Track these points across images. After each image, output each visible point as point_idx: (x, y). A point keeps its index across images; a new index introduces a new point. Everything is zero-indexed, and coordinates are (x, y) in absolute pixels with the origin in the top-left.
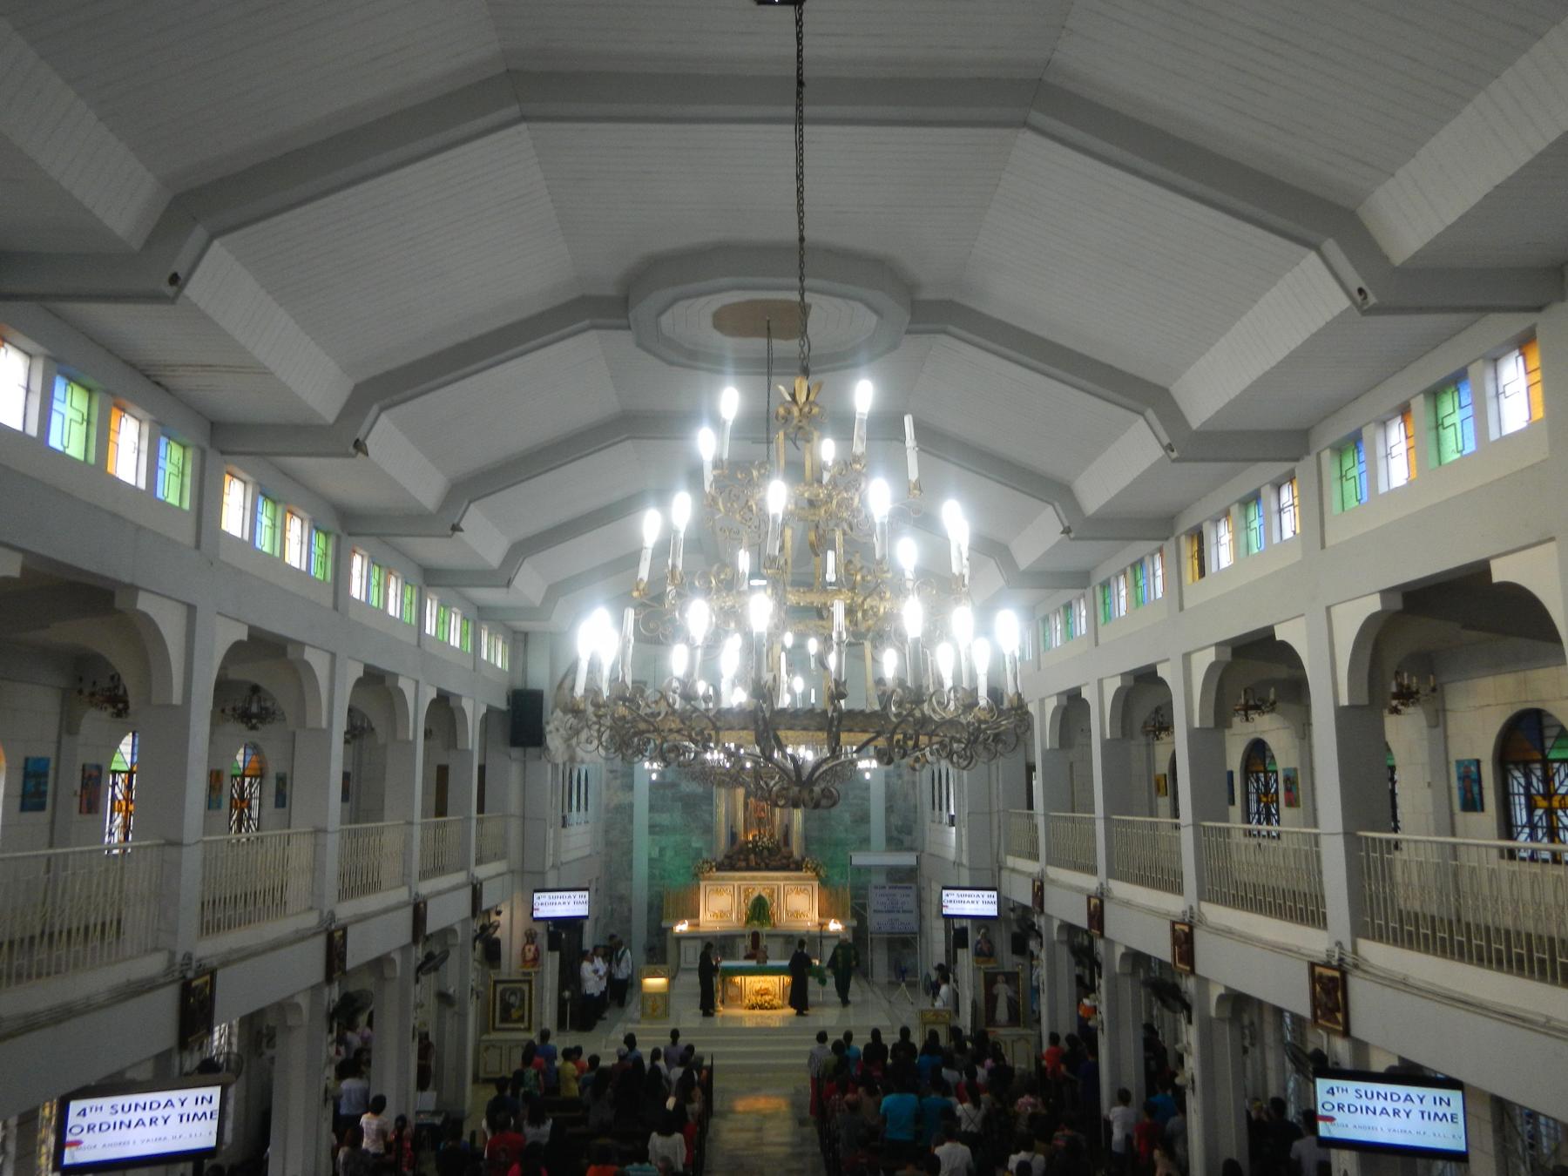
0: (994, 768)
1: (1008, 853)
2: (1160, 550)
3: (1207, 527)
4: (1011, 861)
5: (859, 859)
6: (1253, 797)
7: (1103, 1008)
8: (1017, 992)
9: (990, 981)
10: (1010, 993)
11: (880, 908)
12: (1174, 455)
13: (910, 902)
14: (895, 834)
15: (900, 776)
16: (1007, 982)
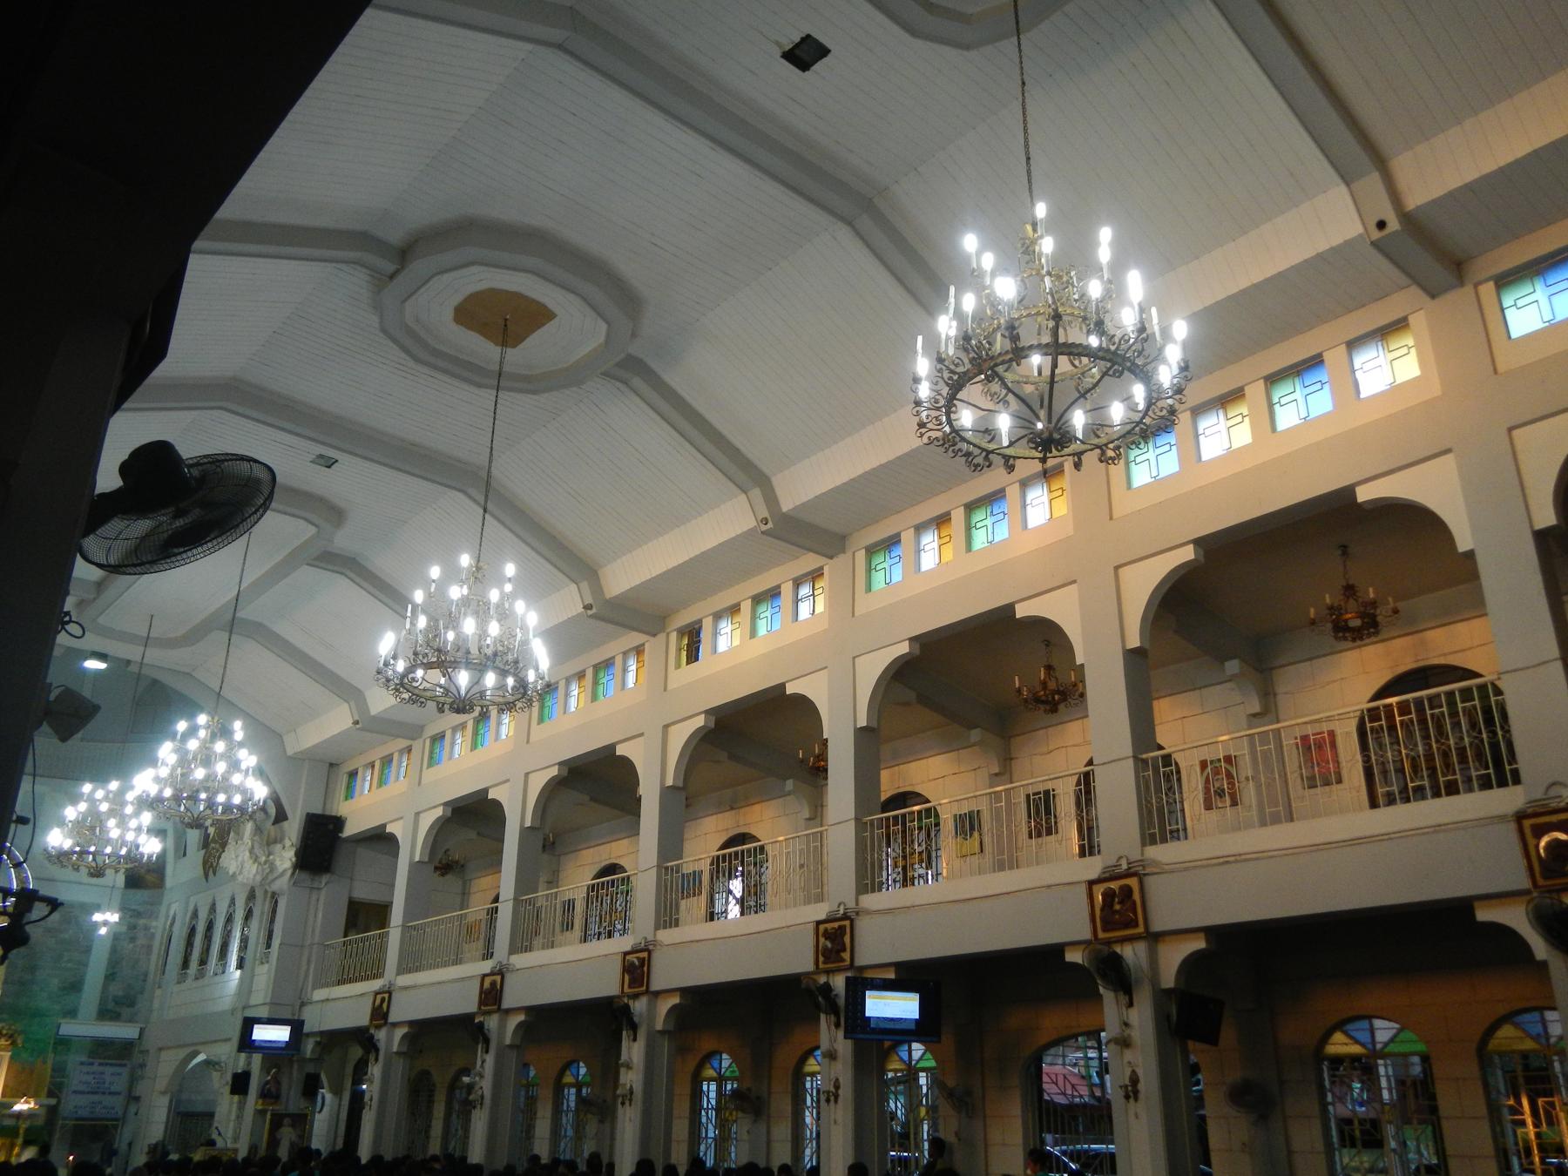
0: (314, 897)
1: (314, 988)
2: (639, 651)
3: (707, 624)
4: (319, 994)
5: (69, 1028)
6: (594, 920)
7: (486, 1085)
8: (301, 1137)
9: (277, 1123)
10: (294, 1138)
11: (82, 1088)
12: (764, 528)
13: (120, 1084)
14: (111, 1006)
15: (133, 939)
16: (293, 1126)
